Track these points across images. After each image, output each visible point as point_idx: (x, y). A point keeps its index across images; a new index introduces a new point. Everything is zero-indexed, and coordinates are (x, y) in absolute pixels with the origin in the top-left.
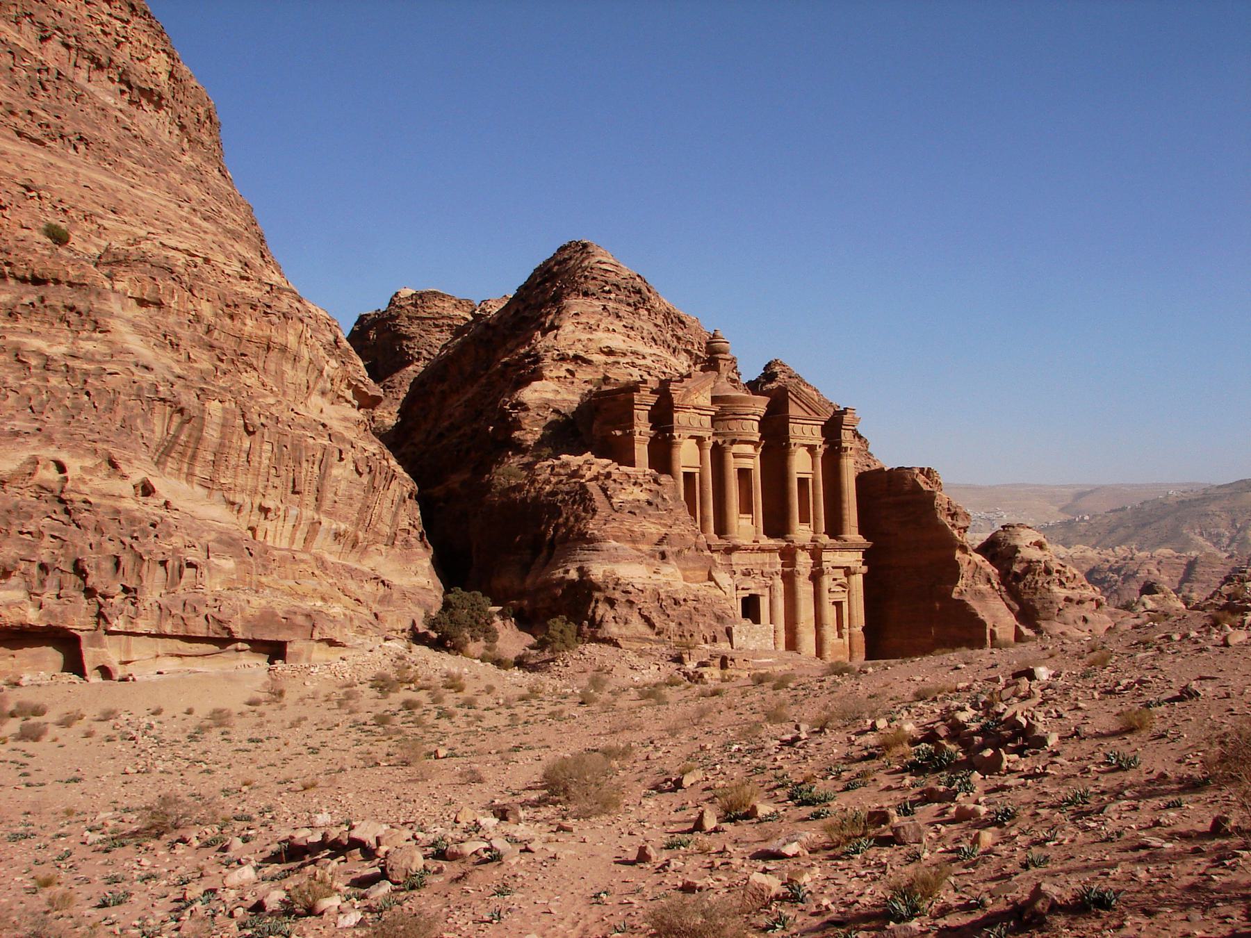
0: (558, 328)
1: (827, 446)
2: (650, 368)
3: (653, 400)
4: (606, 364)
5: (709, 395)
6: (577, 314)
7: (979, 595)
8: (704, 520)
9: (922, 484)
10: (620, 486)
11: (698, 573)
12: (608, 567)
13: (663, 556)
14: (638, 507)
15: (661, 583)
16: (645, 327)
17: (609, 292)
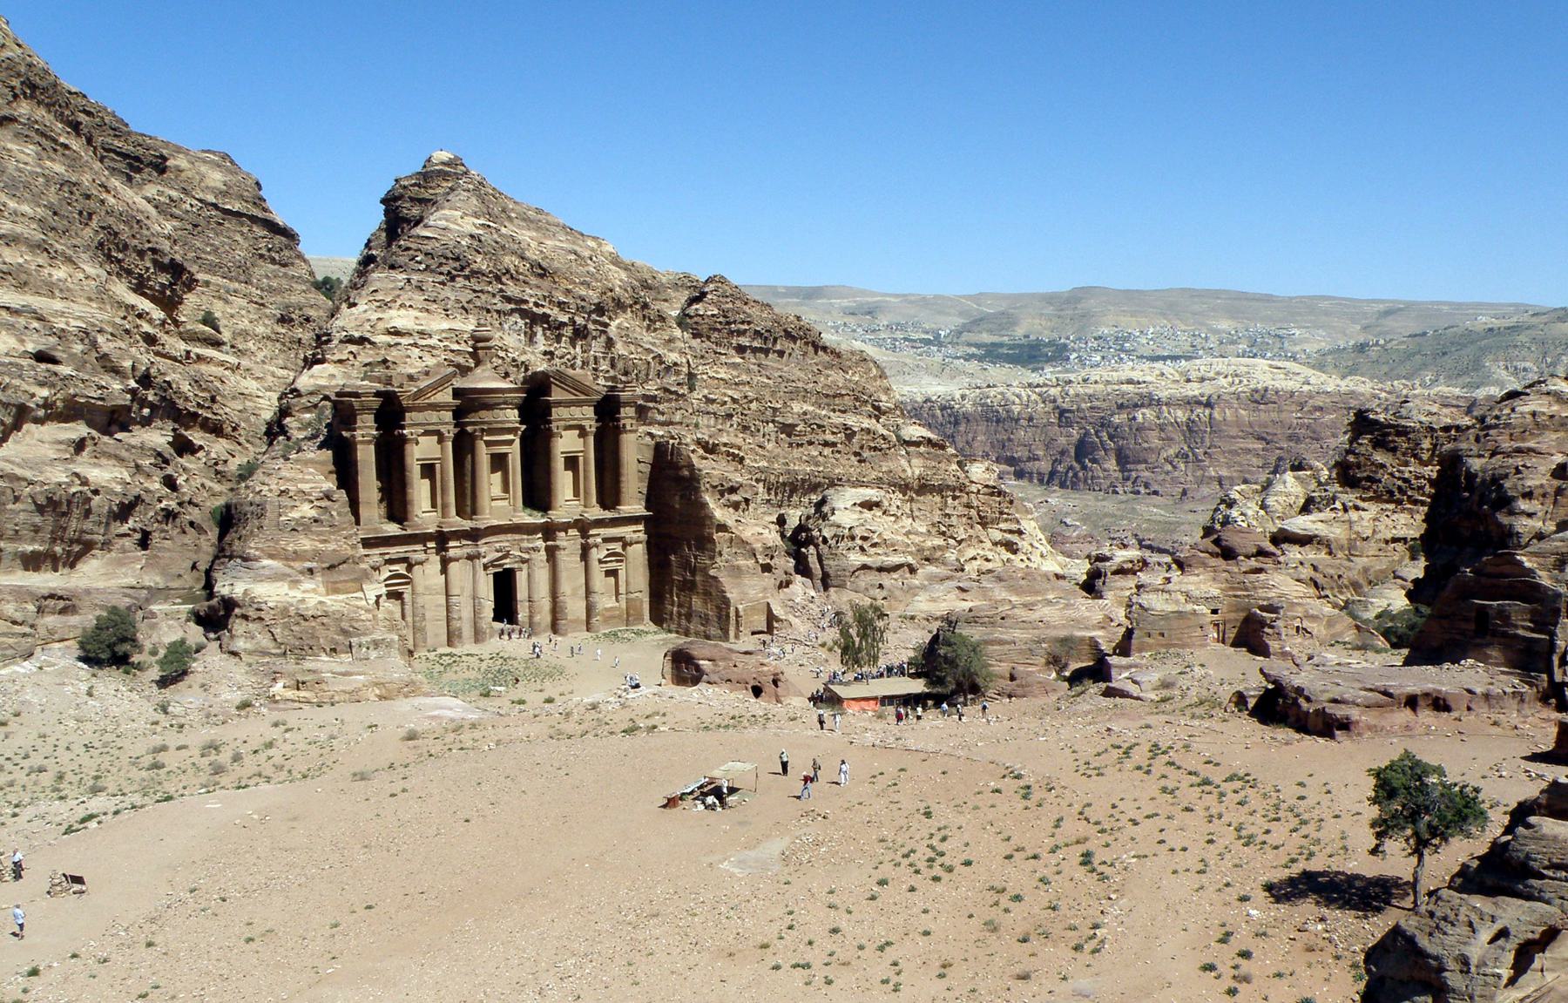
0: (355, 305)
1: (599, 424)
2: (433, 348)
3: (376, 402)
4: (390, 346)
5: (450, 390)
6: (376, 291)
7: (737, 571)
8: (445, 506)
9: (695, 460)
10: (293, 503)
11: (350, 584)
14: (303, 525)
15: (294, 601)
16: (453, 298)
17: (420, 263)
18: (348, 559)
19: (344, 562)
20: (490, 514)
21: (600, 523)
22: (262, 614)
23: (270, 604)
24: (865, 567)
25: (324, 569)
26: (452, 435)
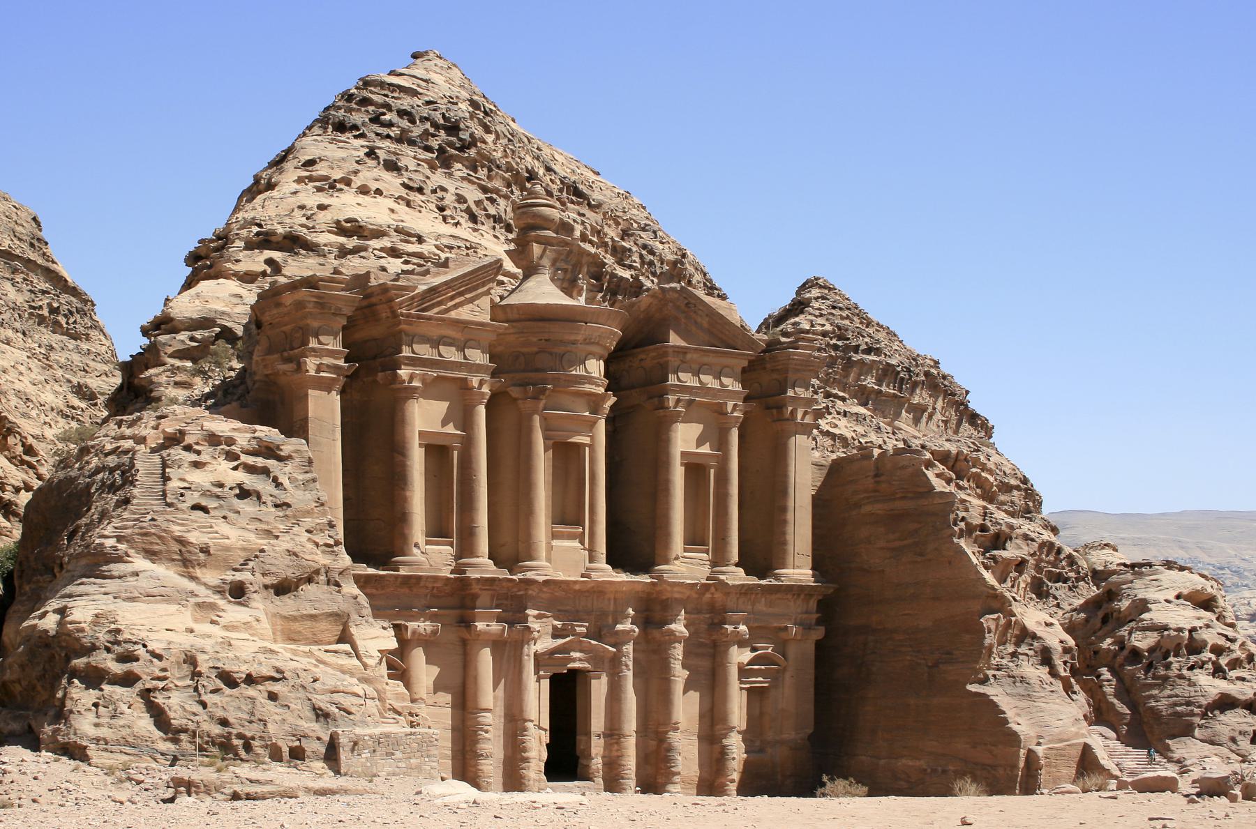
5: (485, 302)
9: (930, 474)
10: (194, 457)
11: (323, 625)
12: (105, 604)
13: (238, 592)
14: (218, 497)
15: (208, 644)
16: (452, 189)
18: (317, 572)
19: (309, 580)
20: (549, 560)
21: (744, 590)
22: (135, 667)
23: (152, 646)
24: (1226, 703)
25: (266, 587)
26: (486, 389)
